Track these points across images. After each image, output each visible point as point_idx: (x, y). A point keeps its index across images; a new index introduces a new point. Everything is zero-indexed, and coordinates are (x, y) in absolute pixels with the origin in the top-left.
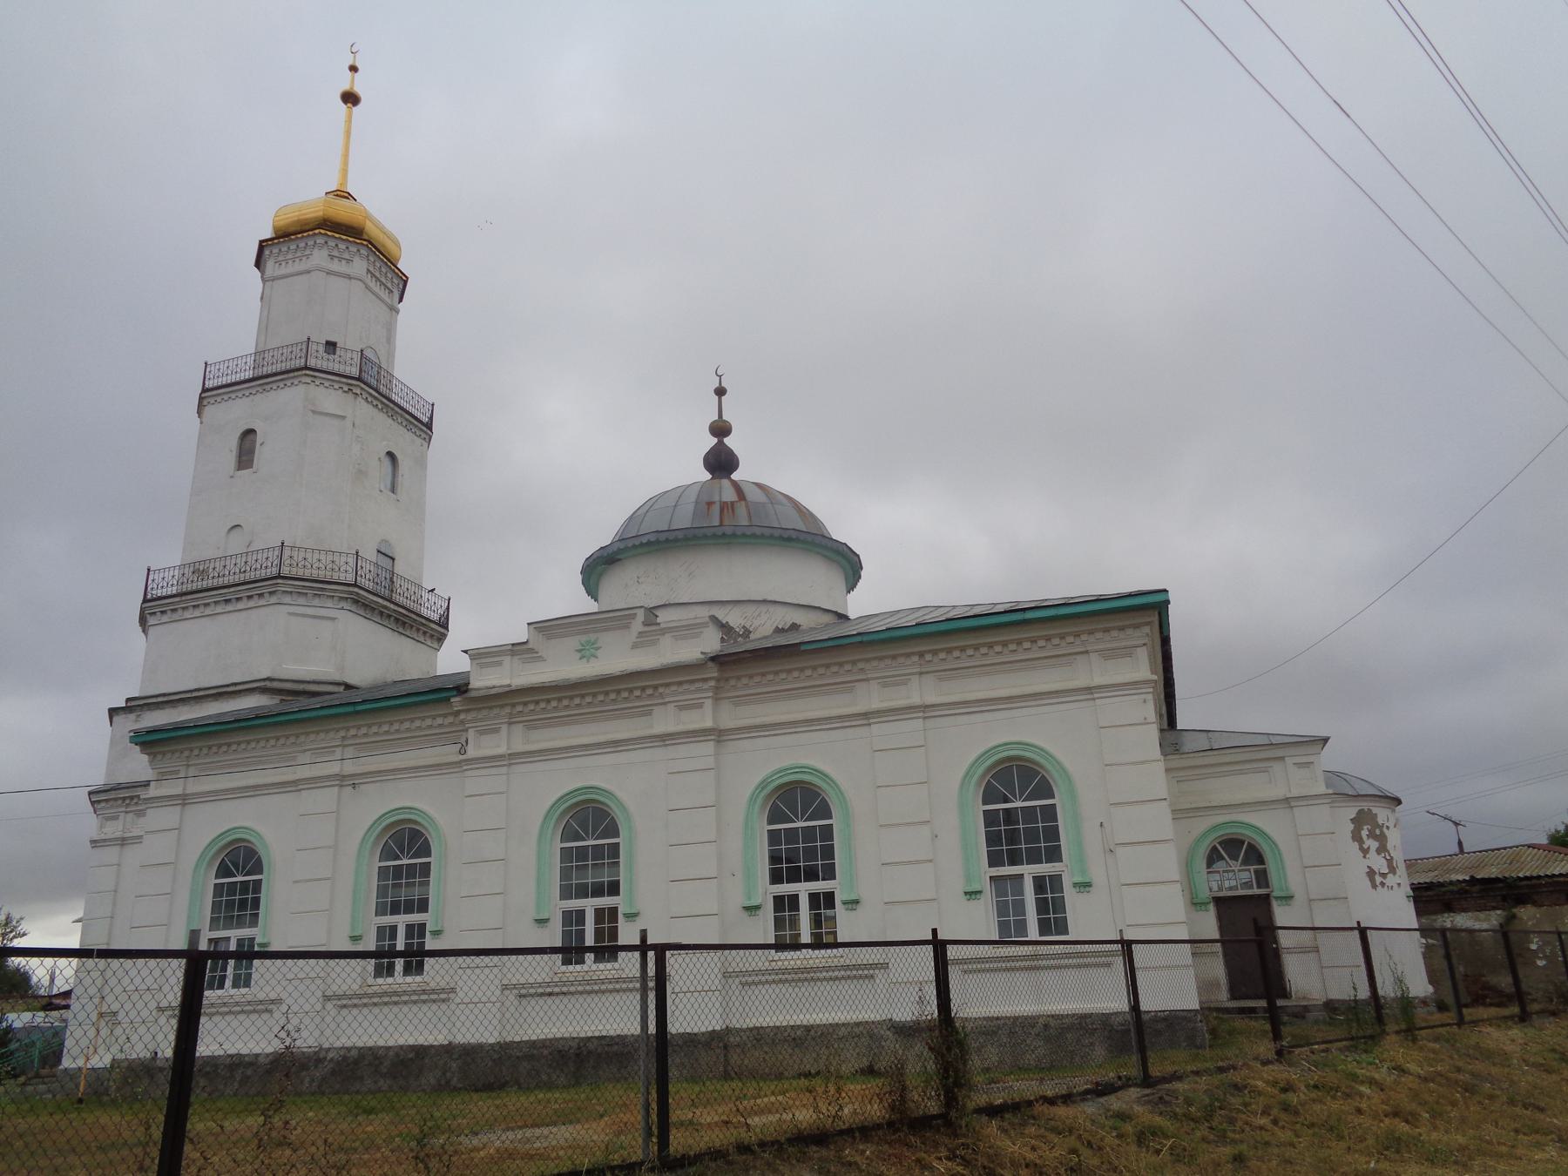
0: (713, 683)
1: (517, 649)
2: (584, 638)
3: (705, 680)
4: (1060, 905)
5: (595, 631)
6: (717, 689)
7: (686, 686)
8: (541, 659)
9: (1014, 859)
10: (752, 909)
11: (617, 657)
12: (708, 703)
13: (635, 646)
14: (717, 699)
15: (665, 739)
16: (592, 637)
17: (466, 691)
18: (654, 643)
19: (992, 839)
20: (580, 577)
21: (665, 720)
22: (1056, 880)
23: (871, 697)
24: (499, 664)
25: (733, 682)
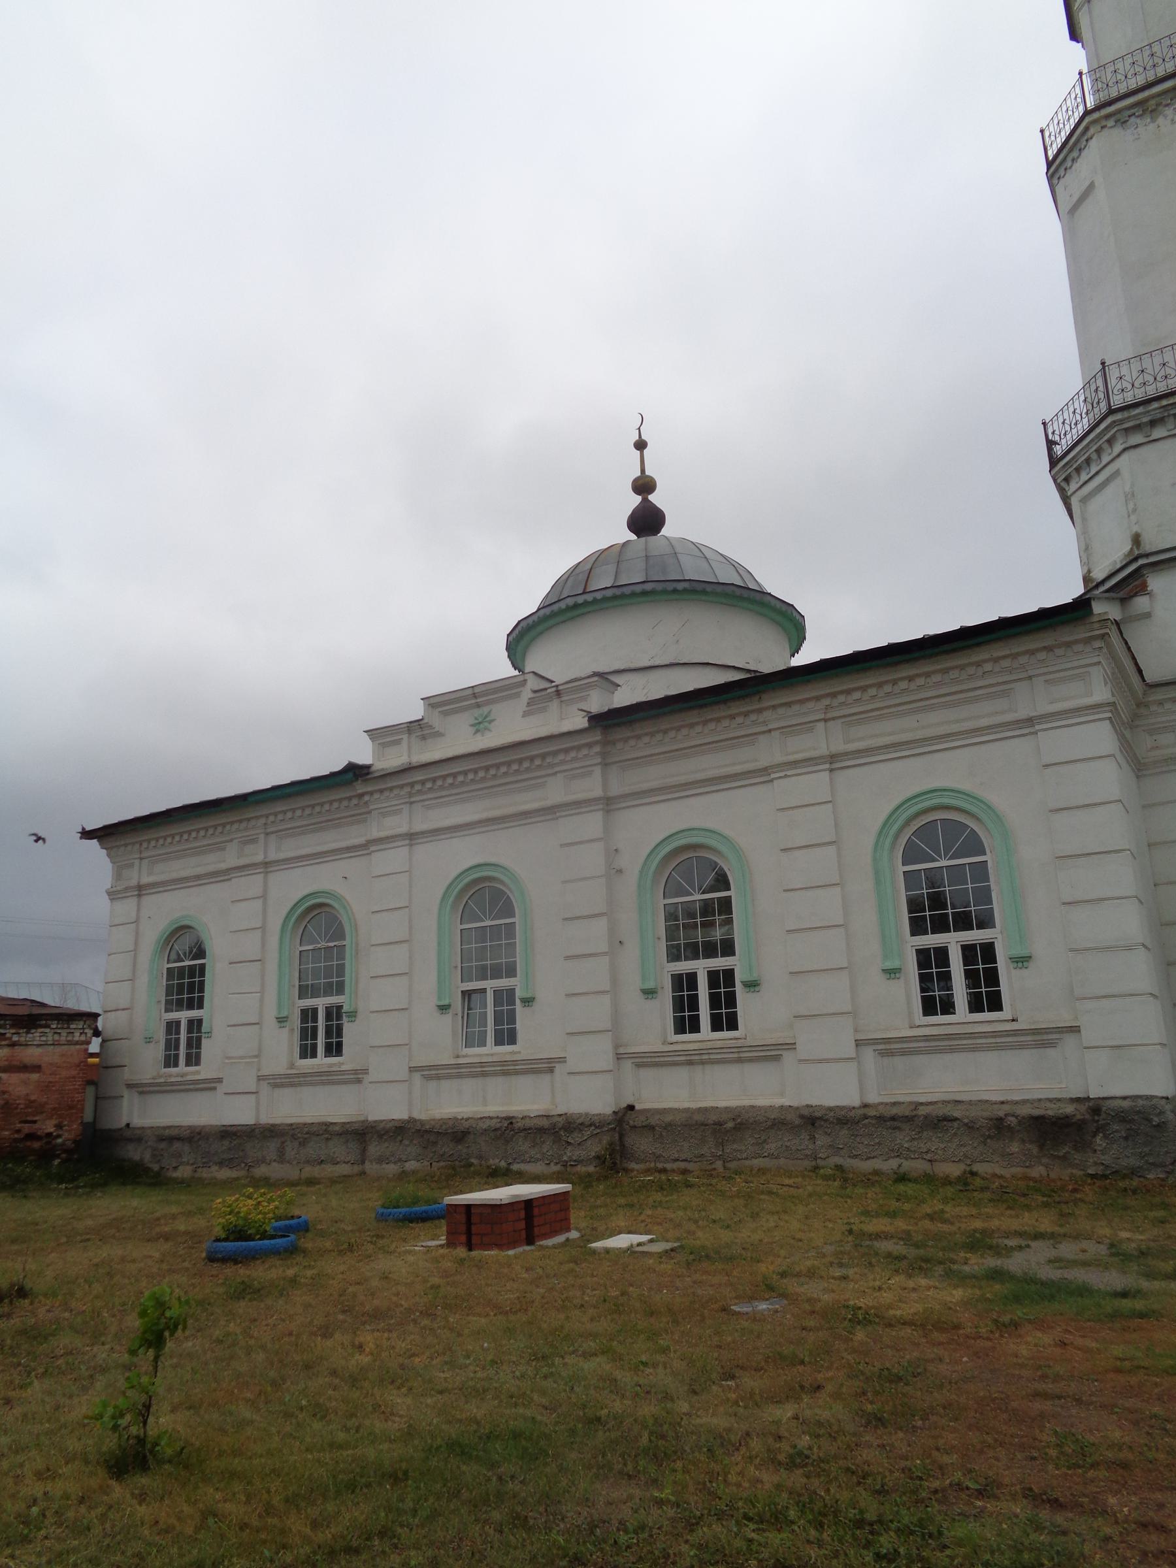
0: (597, 749)
1: (414, 728)
2: (476, 712)
3: (589, 745)
4: (993, 977)
5: (488, 703)
6: (604, 755)
7: (573, 754)
8: (438, 734)
9: (940, 926)
10: (649, 993)
11: (512, 726)
12: (598, 771)
13: (526, 714)
14: (605, 765)
15: (552, 812)
16: (485, 710)
17: (368, 774)
18: (544, 710)
19: (914, 905)
20: (506, 654)
21: (555, 791)
22: (988, 950)
23: (768, 751)
24: (398, 742)
25: (619, 745)
